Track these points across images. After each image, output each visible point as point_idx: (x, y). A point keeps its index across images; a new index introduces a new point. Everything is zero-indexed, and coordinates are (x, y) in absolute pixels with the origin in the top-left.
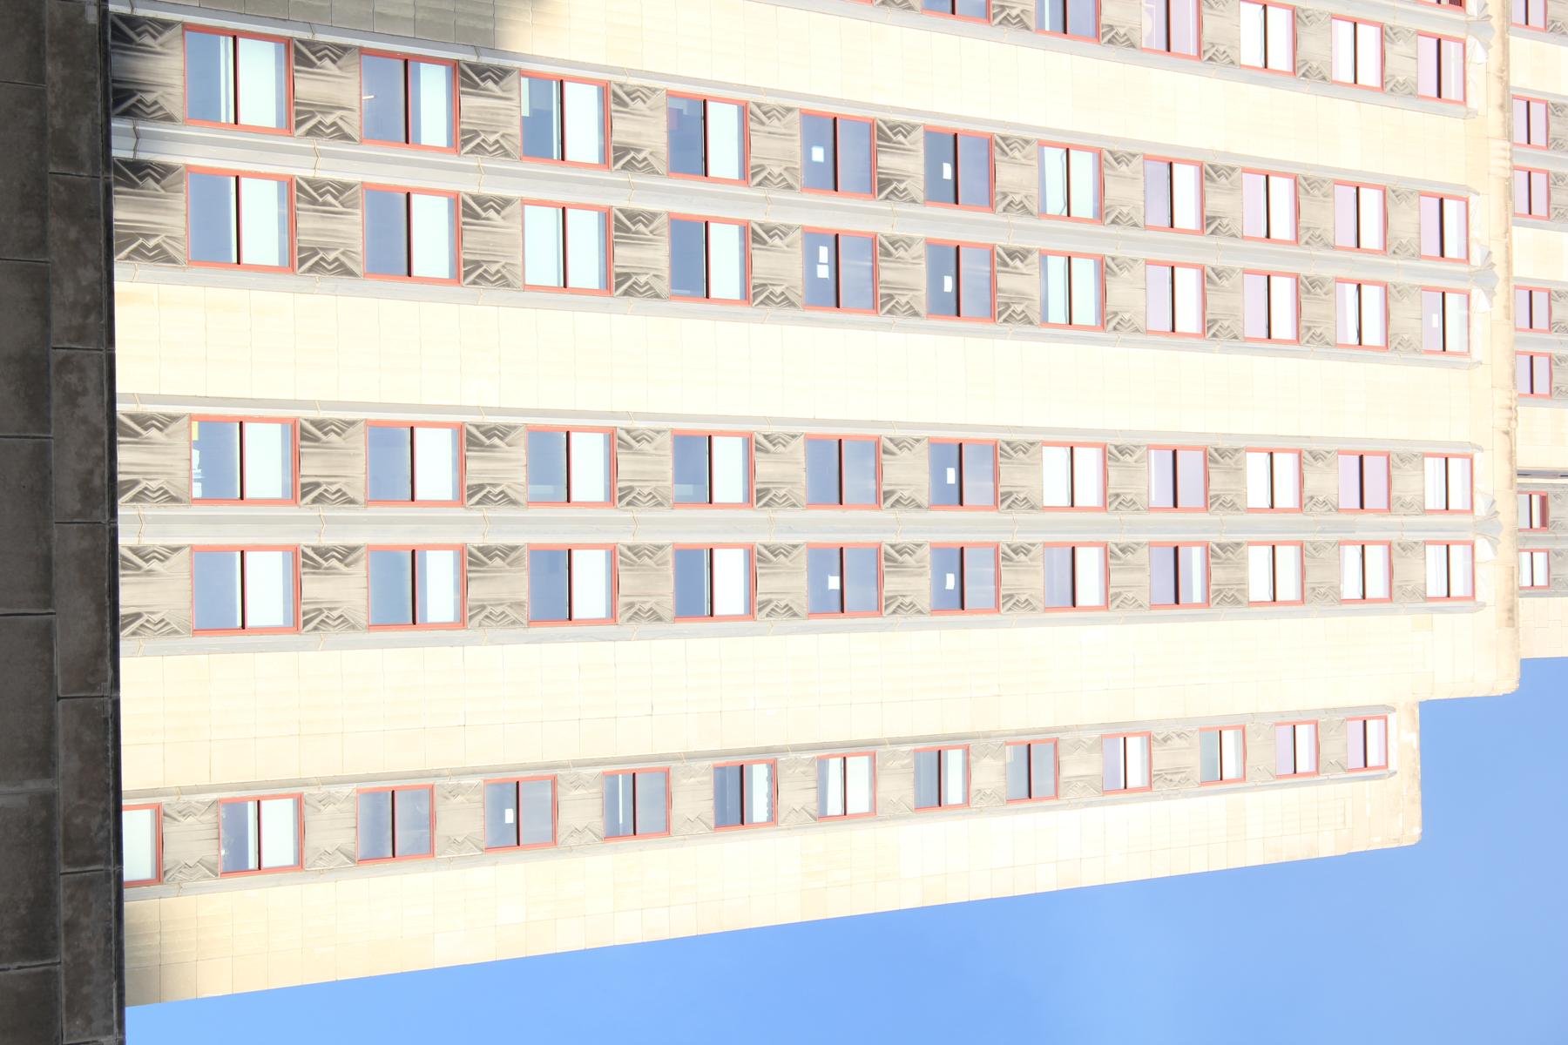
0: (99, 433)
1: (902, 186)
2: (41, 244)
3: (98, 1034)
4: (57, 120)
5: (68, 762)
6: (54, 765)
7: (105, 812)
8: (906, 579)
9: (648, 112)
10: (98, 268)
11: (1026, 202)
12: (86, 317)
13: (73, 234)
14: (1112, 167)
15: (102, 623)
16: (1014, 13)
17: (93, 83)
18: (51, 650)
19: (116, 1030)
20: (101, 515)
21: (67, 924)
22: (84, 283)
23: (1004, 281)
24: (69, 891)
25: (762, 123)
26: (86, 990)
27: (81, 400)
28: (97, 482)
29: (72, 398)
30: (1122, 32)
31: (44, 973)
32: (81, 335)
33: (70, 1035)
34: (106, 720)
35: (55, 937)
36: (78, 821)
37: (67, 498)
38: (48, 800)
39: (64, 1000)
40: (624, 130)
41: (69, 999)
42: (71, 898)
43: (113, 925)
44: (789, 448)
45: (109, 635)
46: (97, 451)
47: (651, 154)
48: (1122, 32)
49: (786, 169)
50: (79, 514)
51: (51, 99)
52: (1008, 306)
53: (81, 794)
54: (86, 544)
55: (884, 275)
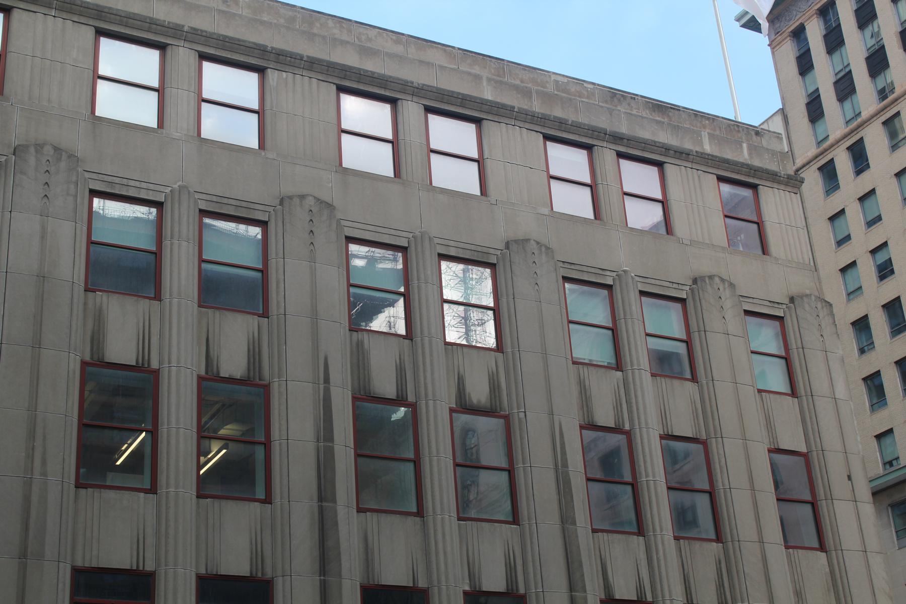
0: (379, 33)
2: (324, 37)
3: (551, 80)
4: (282, 21)
5: (476, 70)
6: (479, 75)
7: (490, 61)
10: (328, 19)
12: (344, 27)
13: (318, 25)
15: (436, 47)
17: (268, 4)
18: (446, 67)
19: (550, 74)
20: (404, 39)
21: (521, 82)
22: (333, 25)
24: (513, 79)
26: (539, 80)
27: (370, 36)
28: (394, 38)
29: (369, 40)
31: (536, 93)
32: (349, 31)
33: (551, 89)
34: (464, 54)
35: (526, 87)
36: (493, 71)
37: (399, 49)
38: (489, 80)
39: (542, 89)
41: (542, 87)
42: (514, 79)
43: (522, 67)
45: (439, 46)
46: (385, 35)
50: (404, 46)
51: (275, 21)
53: (485, 68)
54: (413, 46)
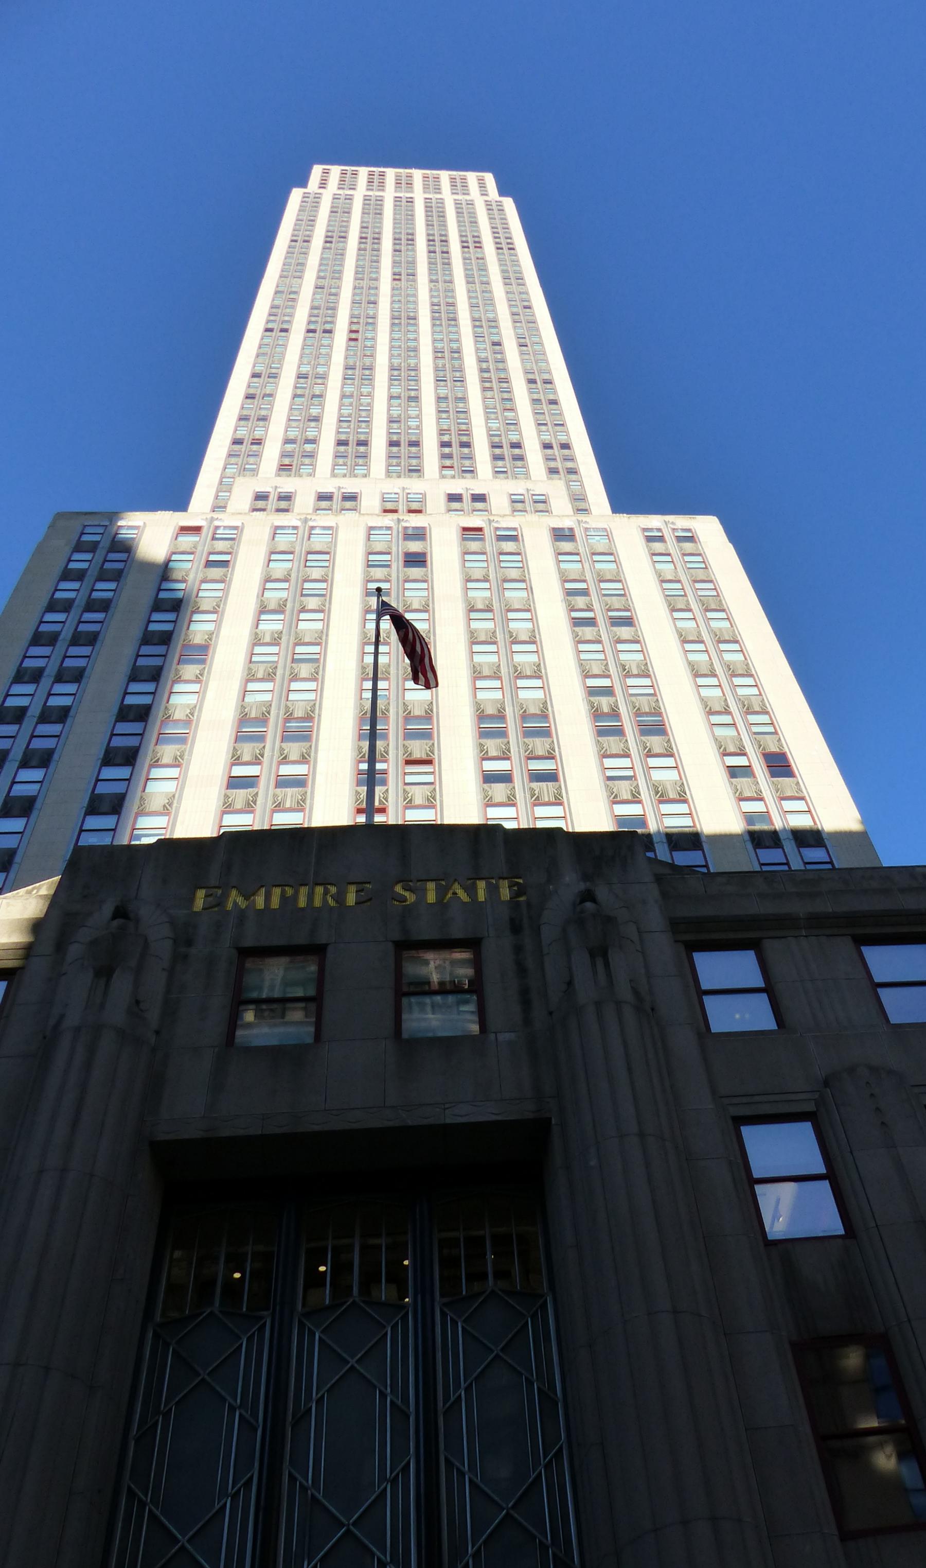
1: (613, 705)
8: (753, 703)
9: (617, 787)
11: (604, 664)
14: (581, 637)
16: (536, 668)
23: (635, 672)
25: (606, 750)
30: (530, 634)
40: (626, 796)
44: (721, 740)
47: (631, 786)
48: (530, 634)
49: (621, 742)
52: (643, 671)
55: (647, 710)
